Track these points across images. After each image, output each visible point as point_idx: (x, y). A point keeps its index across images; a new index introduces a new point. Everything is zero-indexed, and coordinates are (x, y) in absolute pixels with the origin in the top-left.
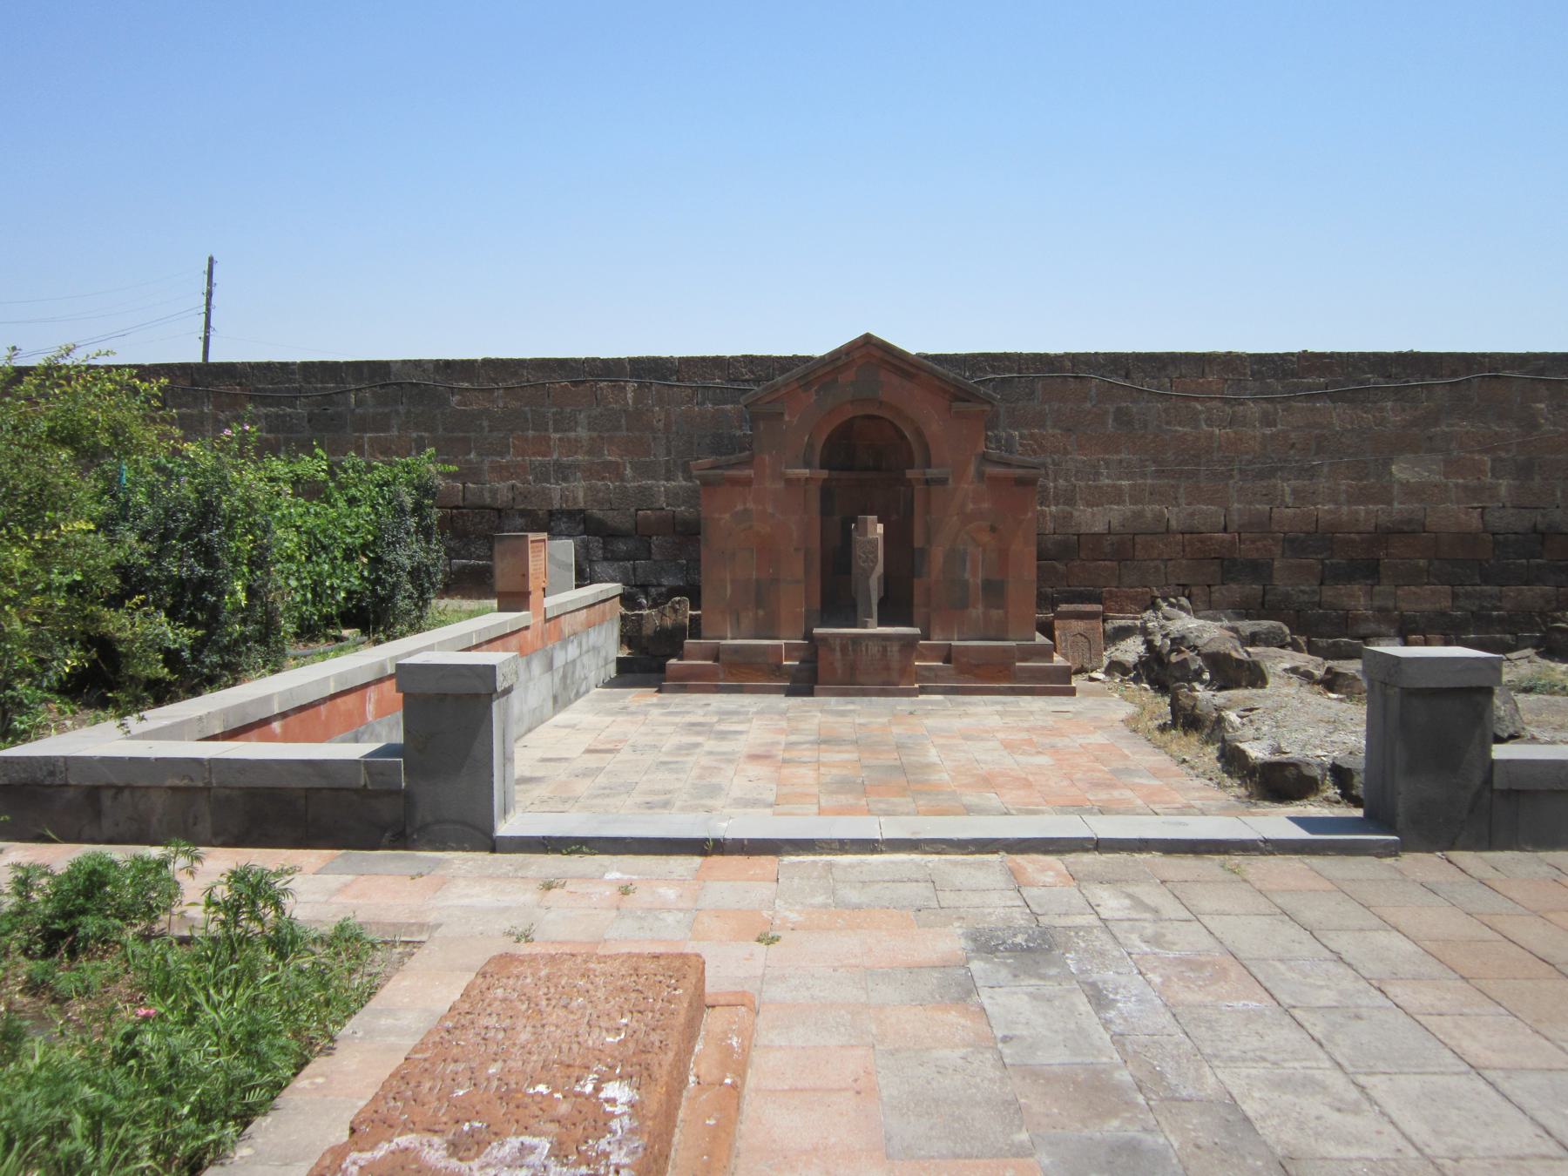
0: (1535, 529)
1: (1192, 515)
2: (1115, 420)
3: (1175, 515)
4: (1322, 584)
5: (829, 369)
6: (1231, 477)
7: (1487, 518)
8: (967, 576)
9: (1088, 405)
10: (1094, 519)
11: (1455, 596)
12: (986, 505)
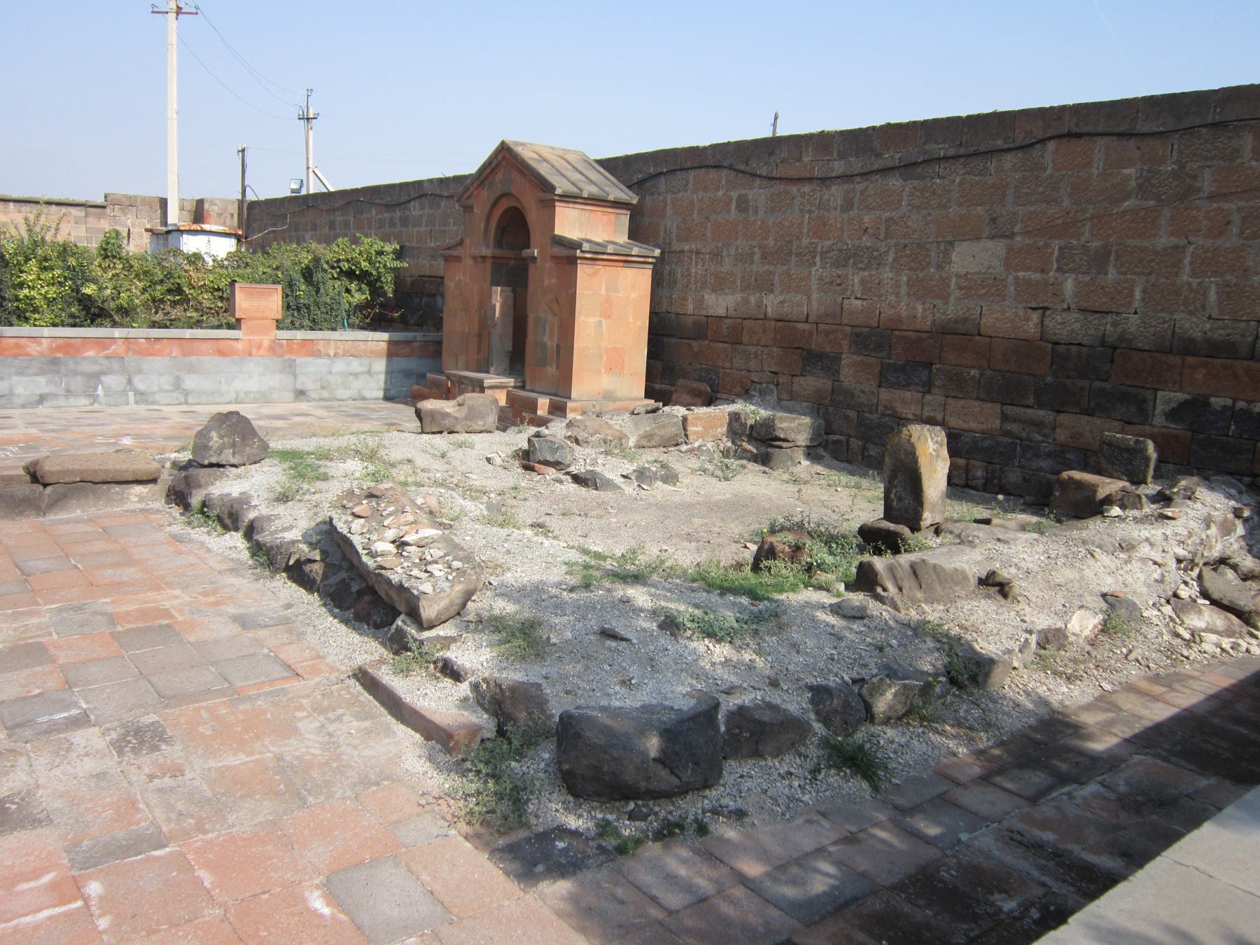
0: (1103, 343)
1: (782, 302)
2: (737, 207)
3: (772, 303)
4: (879, 386)
5: (488, 171)
6: (814, 264)
7: (1047, 322)
8: (546, 339)
9: (720, 193)
10: (720, 304)
11: (1005, 418)
12: (554, 281)
